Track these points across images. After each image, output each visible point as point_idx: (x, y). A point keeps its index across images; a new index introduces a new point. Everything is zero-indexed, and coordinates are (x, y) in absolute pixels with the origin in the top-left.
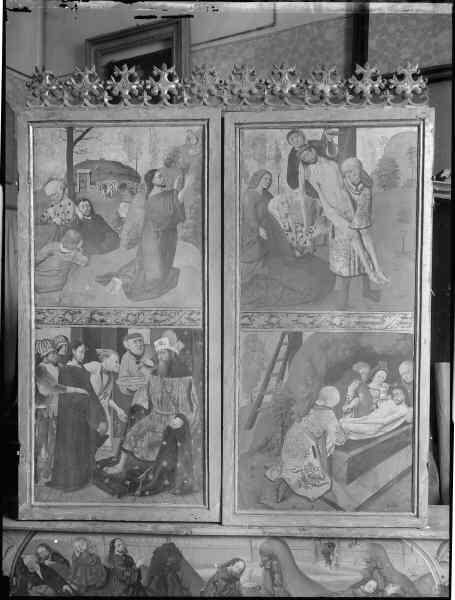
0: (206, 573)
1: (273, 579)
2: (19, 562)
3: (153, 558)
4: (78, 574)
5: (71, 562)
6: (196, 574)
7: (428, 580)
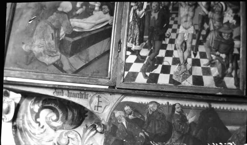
4: (150, 126)
6: (227, 129)
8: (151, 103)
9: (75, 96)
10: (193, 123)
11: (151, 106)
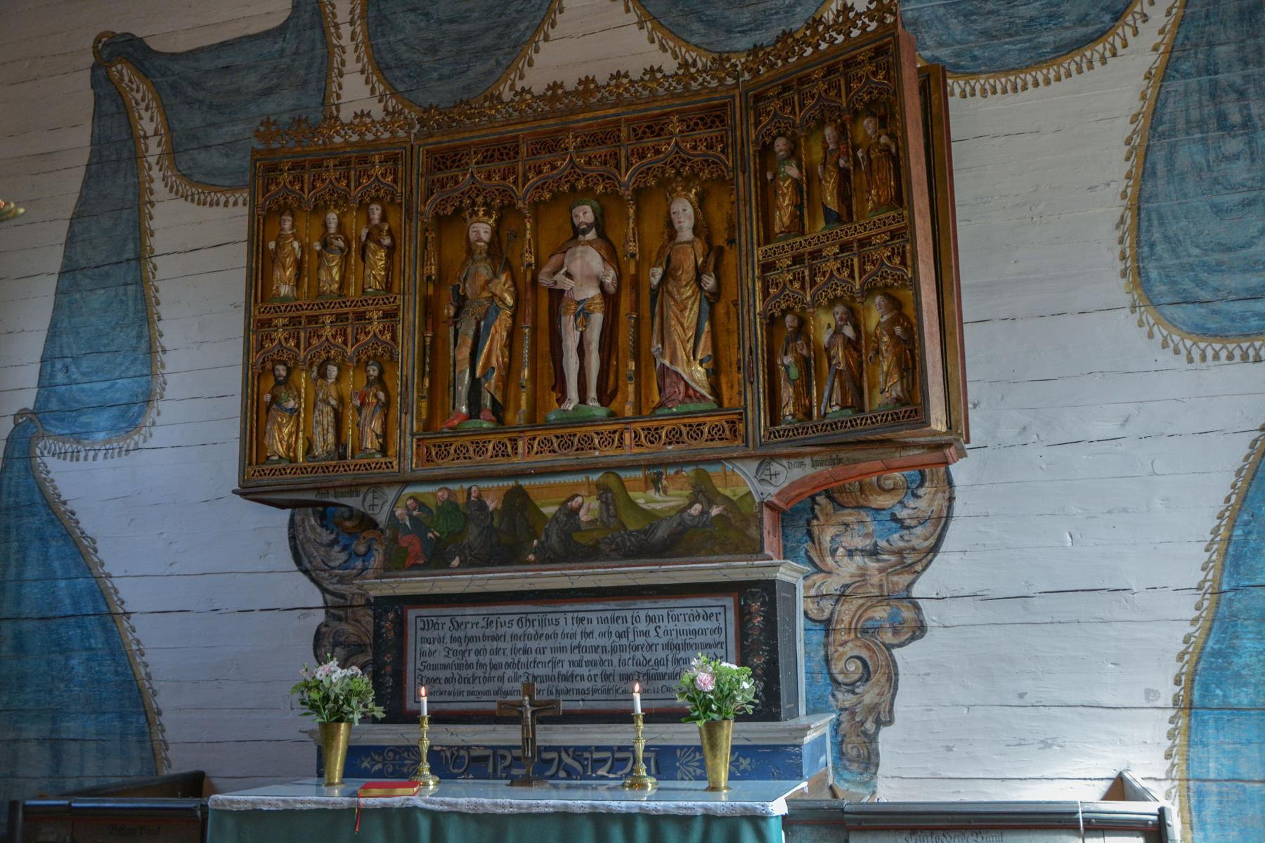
0: (549, 510)
1: (608, 510)
2: (392, 513)
3: (503, 502)
5: (434, 511)
6: (541, 512)
7: (748, 499)
8: (440, 490)
9: (343, 495)
10: (495, 509)
11: (440, 494)
